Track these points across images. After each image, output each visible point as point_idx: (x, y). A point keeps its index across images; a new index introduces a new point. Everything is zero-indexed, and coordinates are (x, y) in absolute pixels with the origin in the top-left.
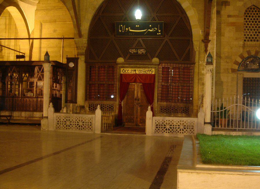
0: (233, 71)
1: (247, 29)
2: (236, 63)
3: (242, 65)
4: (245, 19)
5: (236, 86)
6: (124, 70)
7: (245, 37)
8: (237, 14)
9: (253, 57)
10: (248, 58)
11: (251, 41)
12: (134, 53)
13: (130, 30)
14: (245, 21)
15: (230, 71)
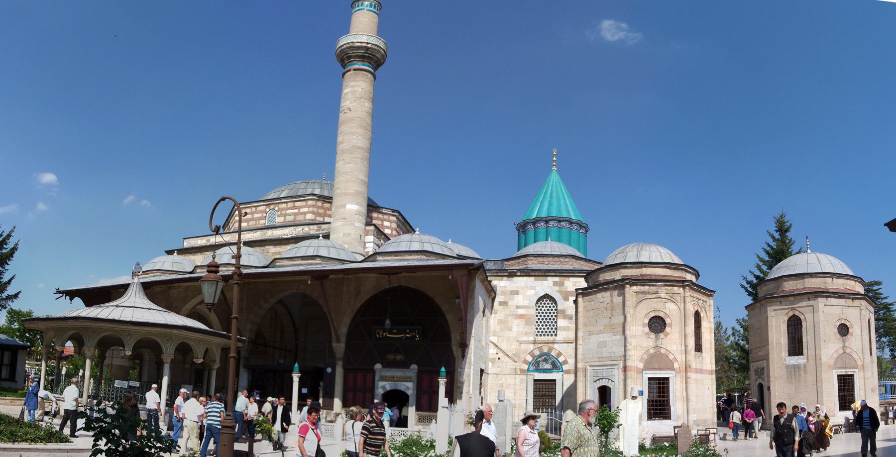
0: (522, 371)
1: (539, 321)
2: (525, 362)
3: (532, 365)
4: (537, 310)
5: (526, 388)
6: (381, 376)
7: (537, 331)
8: (527, 305)
9: (546, 355)
10: (540, 356)
11: (544, 335)
12: (392, 359)
13: (388, 335)
14: (537, 312)
15: (519, 372)
